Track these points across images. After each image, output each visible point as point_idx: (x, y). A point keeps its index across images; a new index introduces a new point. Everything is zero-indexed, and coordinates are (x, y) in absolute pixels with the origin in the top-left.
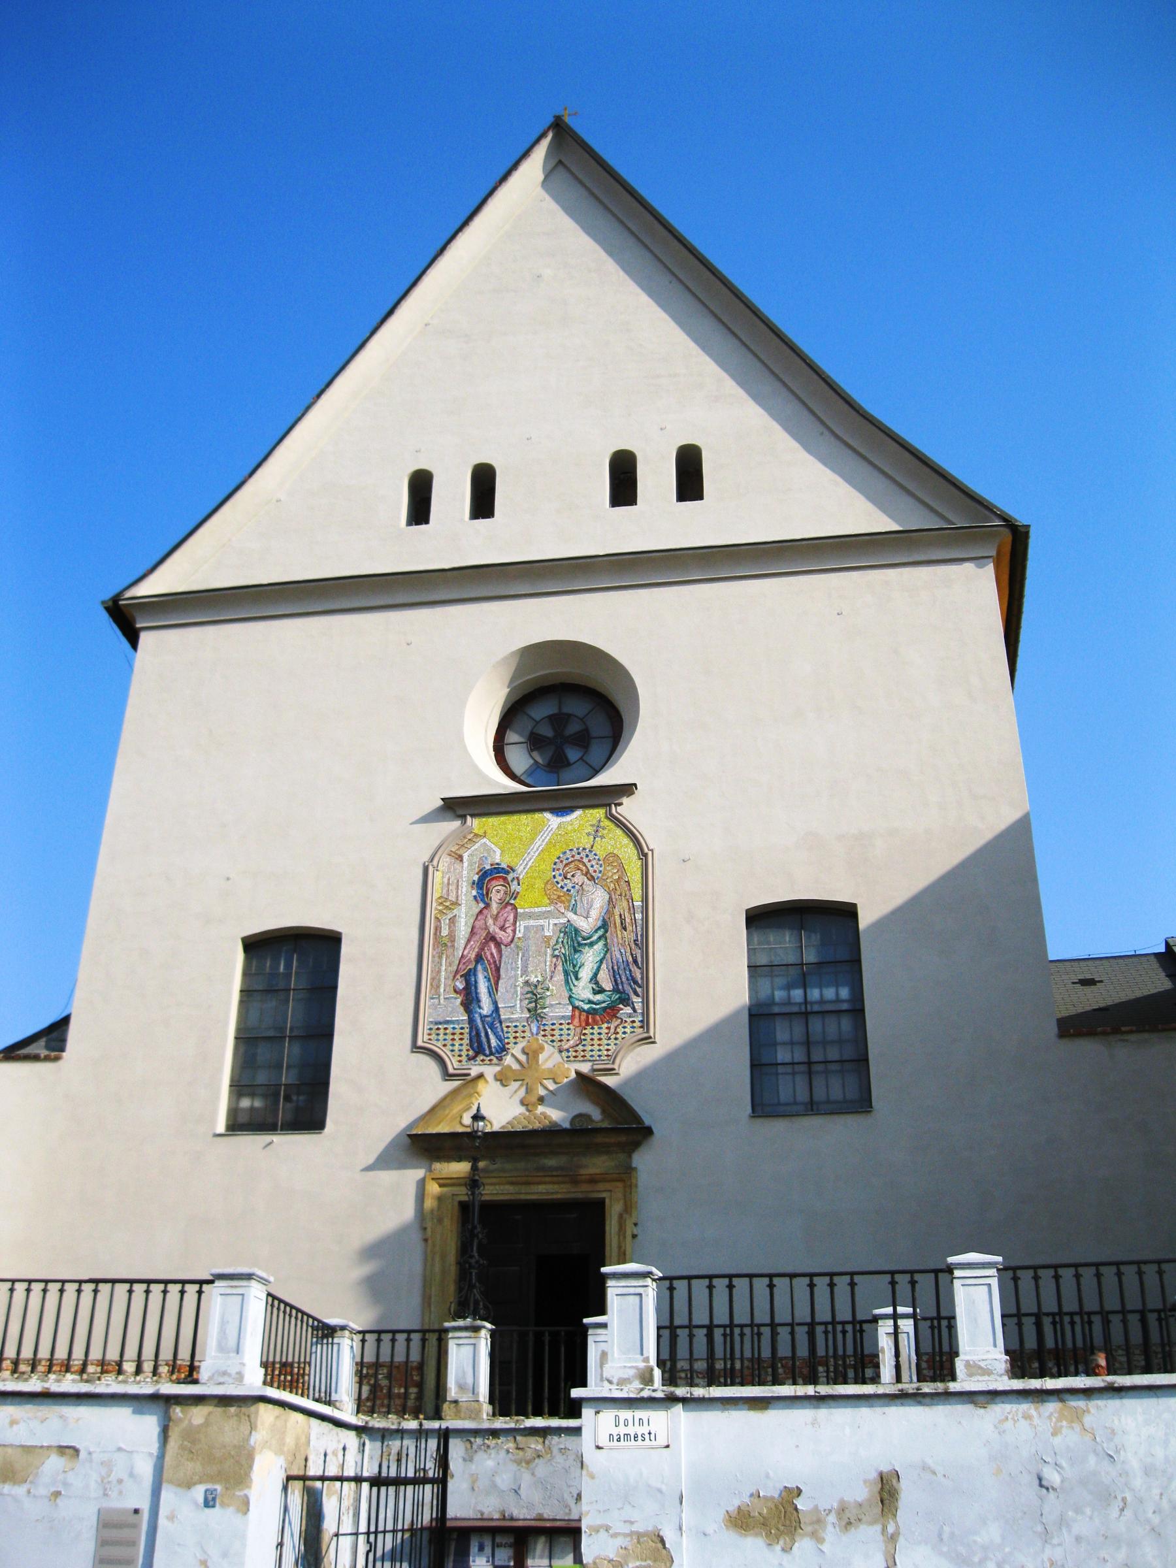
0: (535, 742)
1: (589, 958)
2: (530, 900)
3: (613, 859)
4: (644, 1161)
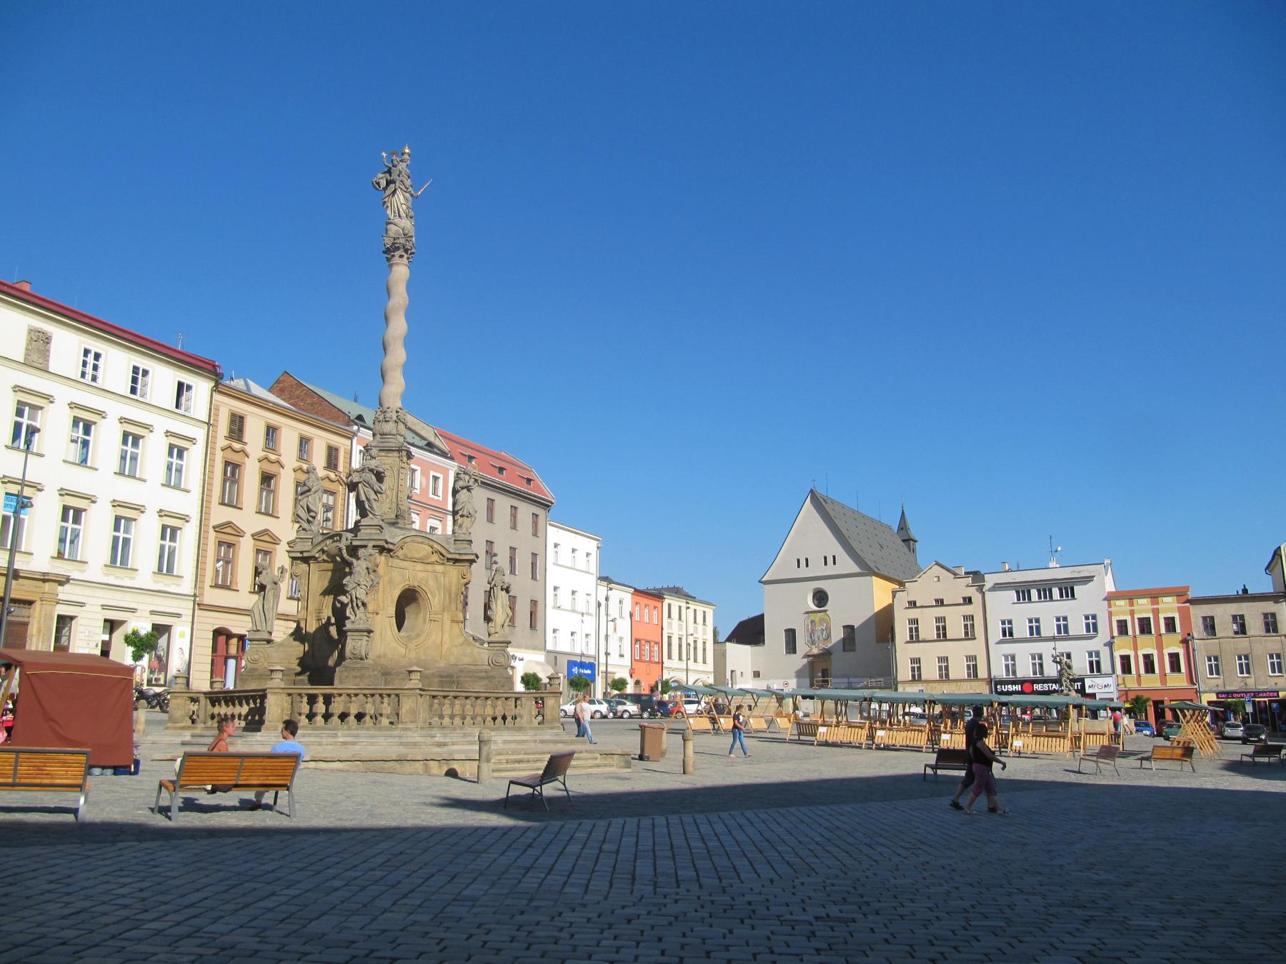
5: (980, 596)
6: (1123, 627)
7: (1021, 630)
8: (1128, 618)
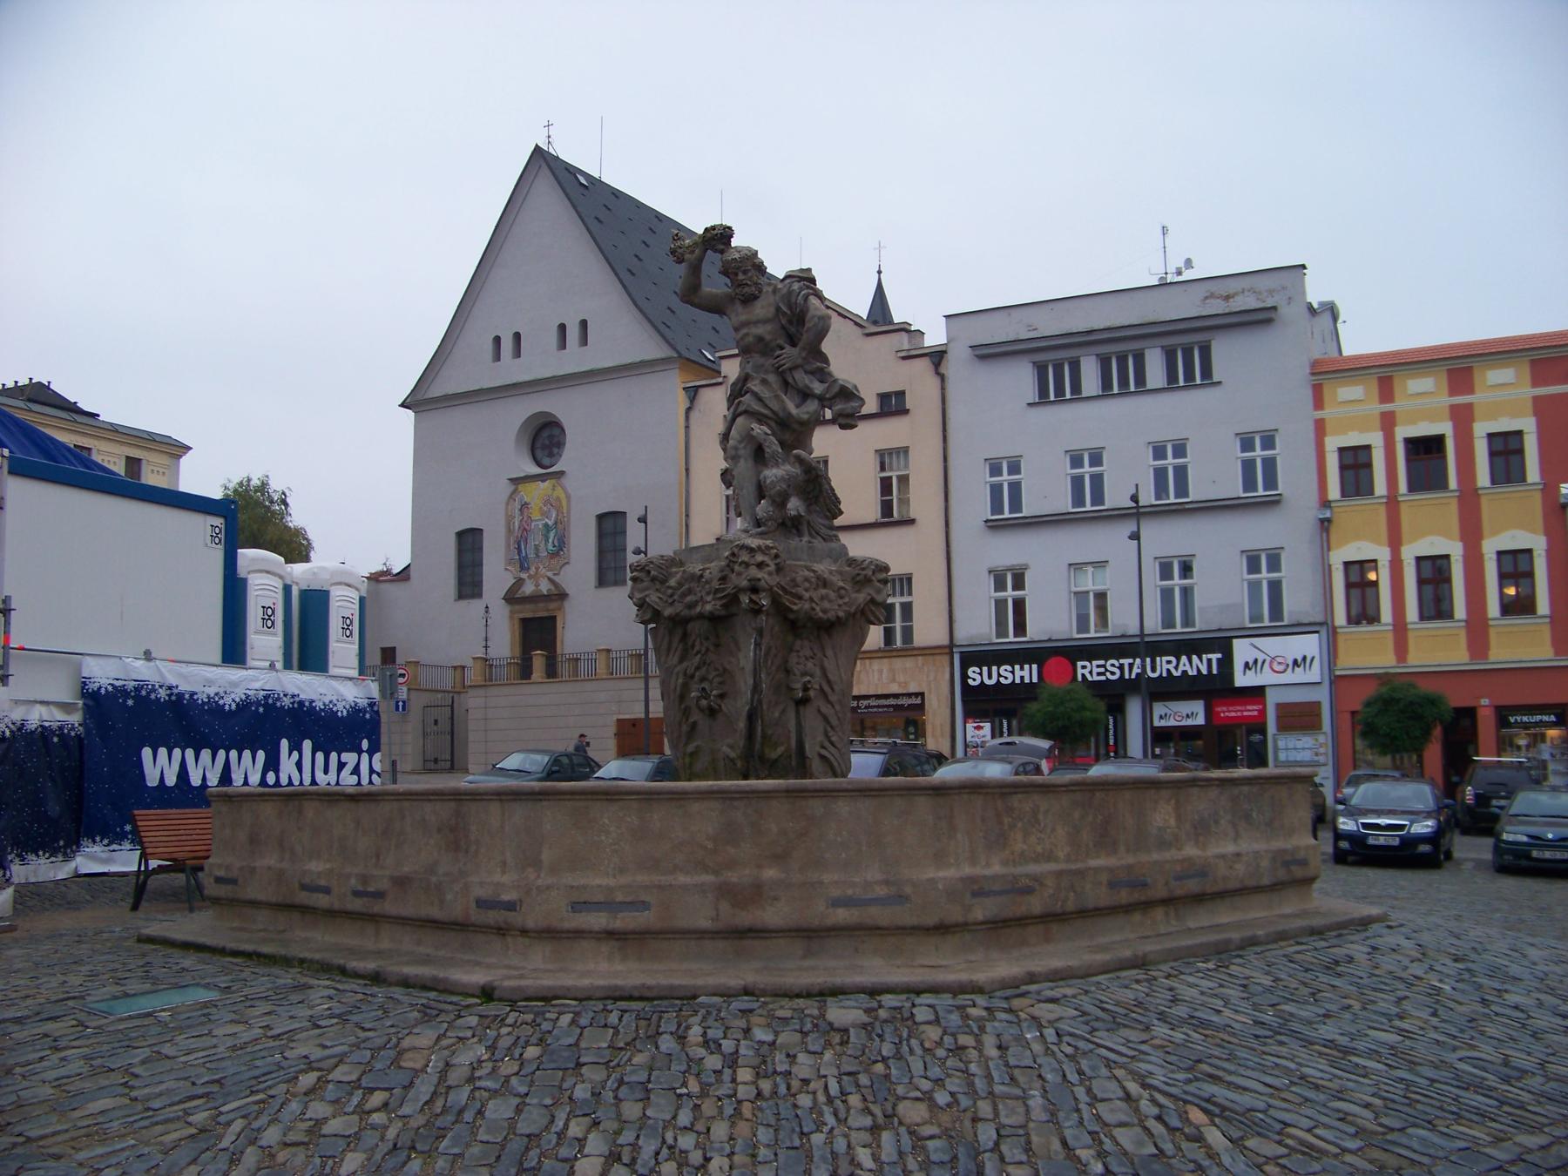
0: (544, 447)
1: (552, 534)
2: (536, 515)
3: (558, 499)
4: (566, 604)
5: (934, 382)
6: (1355, 463)
7: (1046, 490)
8: (1375, 439)
